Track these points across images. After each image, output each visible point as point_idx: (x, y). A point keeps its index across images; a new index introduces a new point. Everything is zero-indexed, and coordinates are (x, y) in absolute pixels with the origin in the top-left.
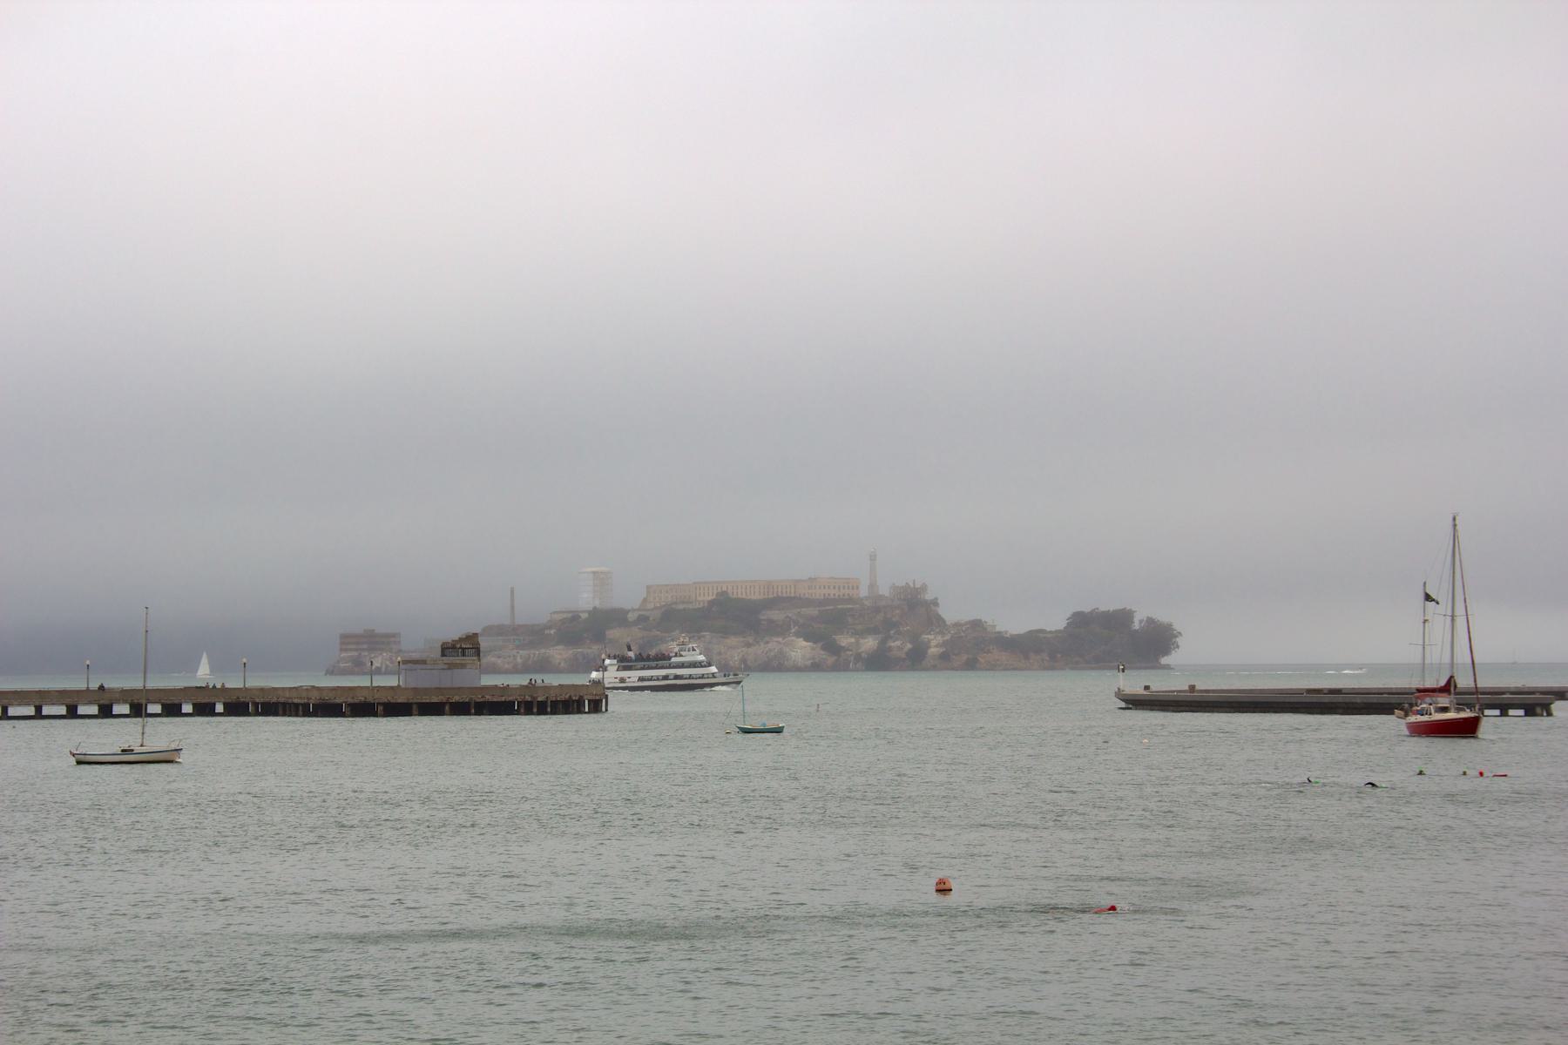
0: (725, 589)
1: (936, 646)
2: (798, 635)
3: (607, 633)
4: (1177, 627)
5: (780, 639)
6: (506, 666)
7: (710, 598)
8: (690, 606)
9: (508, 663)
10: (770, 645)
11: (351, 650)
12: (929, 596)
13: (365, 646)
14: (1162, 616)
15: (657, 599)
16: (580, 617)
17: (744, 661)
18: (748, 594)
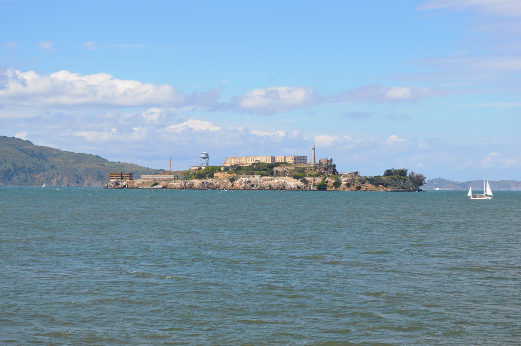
0: (258, 159)
1: (345, 181)
2: (289, 176)
3: (214, 174)
4: (425, 175)
5: (284, 178)
6: (178, 186)
7: (253, 162)
8: (244, 165)
9: (179, 185)
10: (280, 180)
11: (114, 179)
12: (333, 163)
13: (120, 178)
14: (417, 172)
15: (230, 163)
16: (202, 168)
17: (270, 186)
18: (267, 161)
